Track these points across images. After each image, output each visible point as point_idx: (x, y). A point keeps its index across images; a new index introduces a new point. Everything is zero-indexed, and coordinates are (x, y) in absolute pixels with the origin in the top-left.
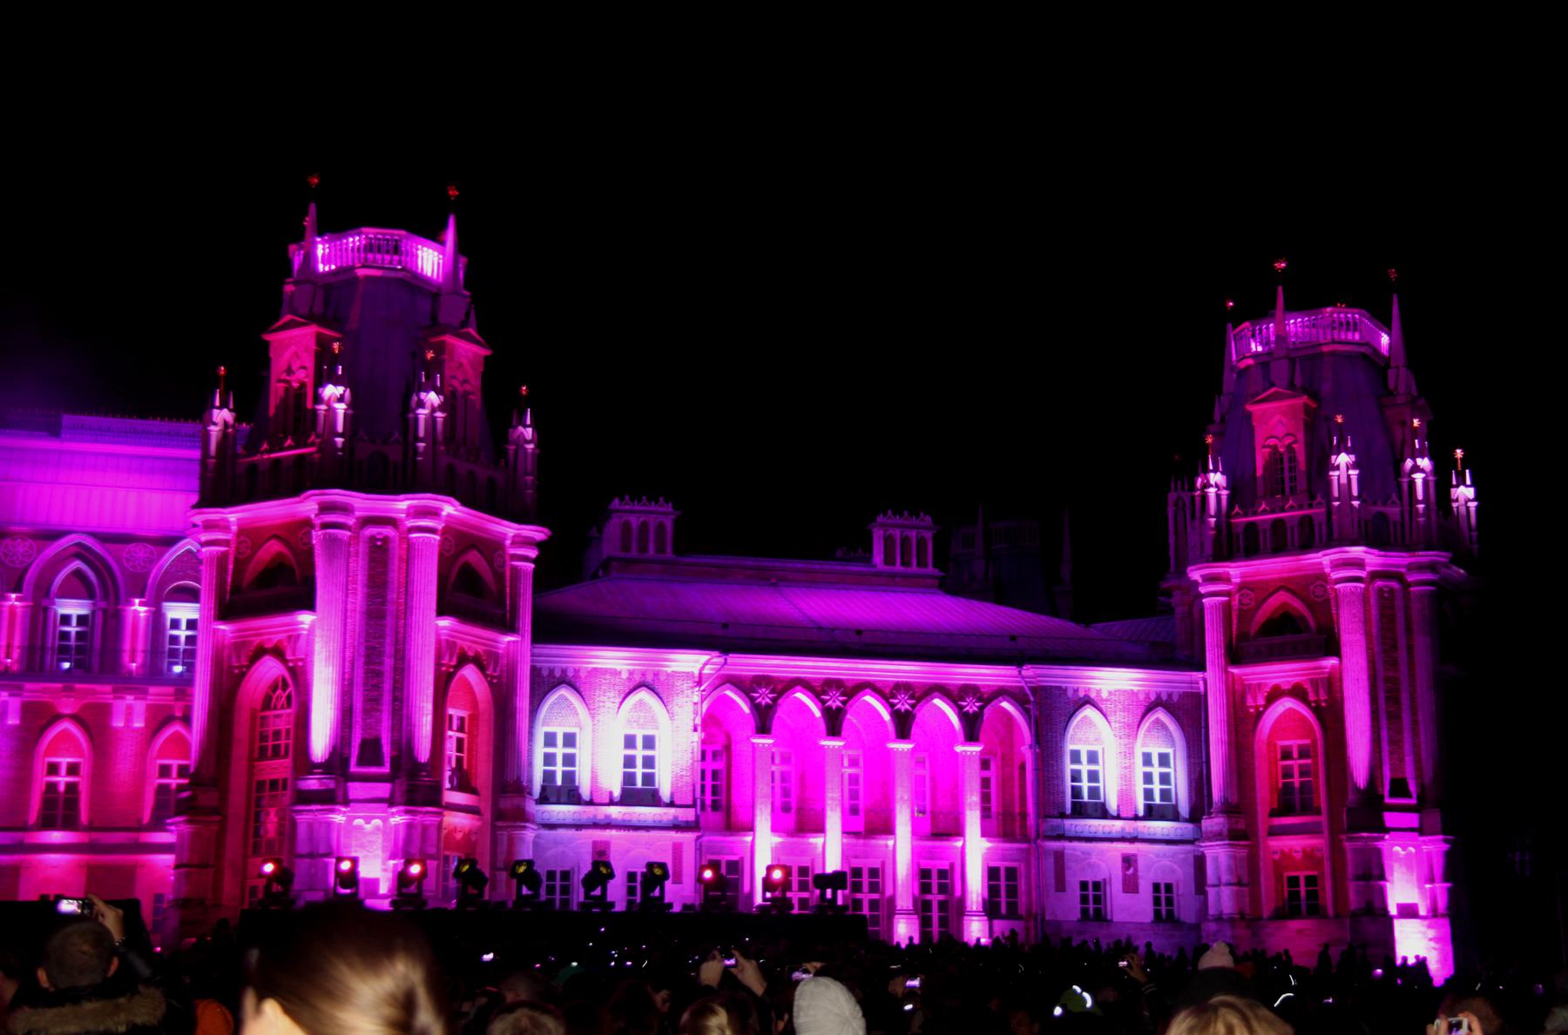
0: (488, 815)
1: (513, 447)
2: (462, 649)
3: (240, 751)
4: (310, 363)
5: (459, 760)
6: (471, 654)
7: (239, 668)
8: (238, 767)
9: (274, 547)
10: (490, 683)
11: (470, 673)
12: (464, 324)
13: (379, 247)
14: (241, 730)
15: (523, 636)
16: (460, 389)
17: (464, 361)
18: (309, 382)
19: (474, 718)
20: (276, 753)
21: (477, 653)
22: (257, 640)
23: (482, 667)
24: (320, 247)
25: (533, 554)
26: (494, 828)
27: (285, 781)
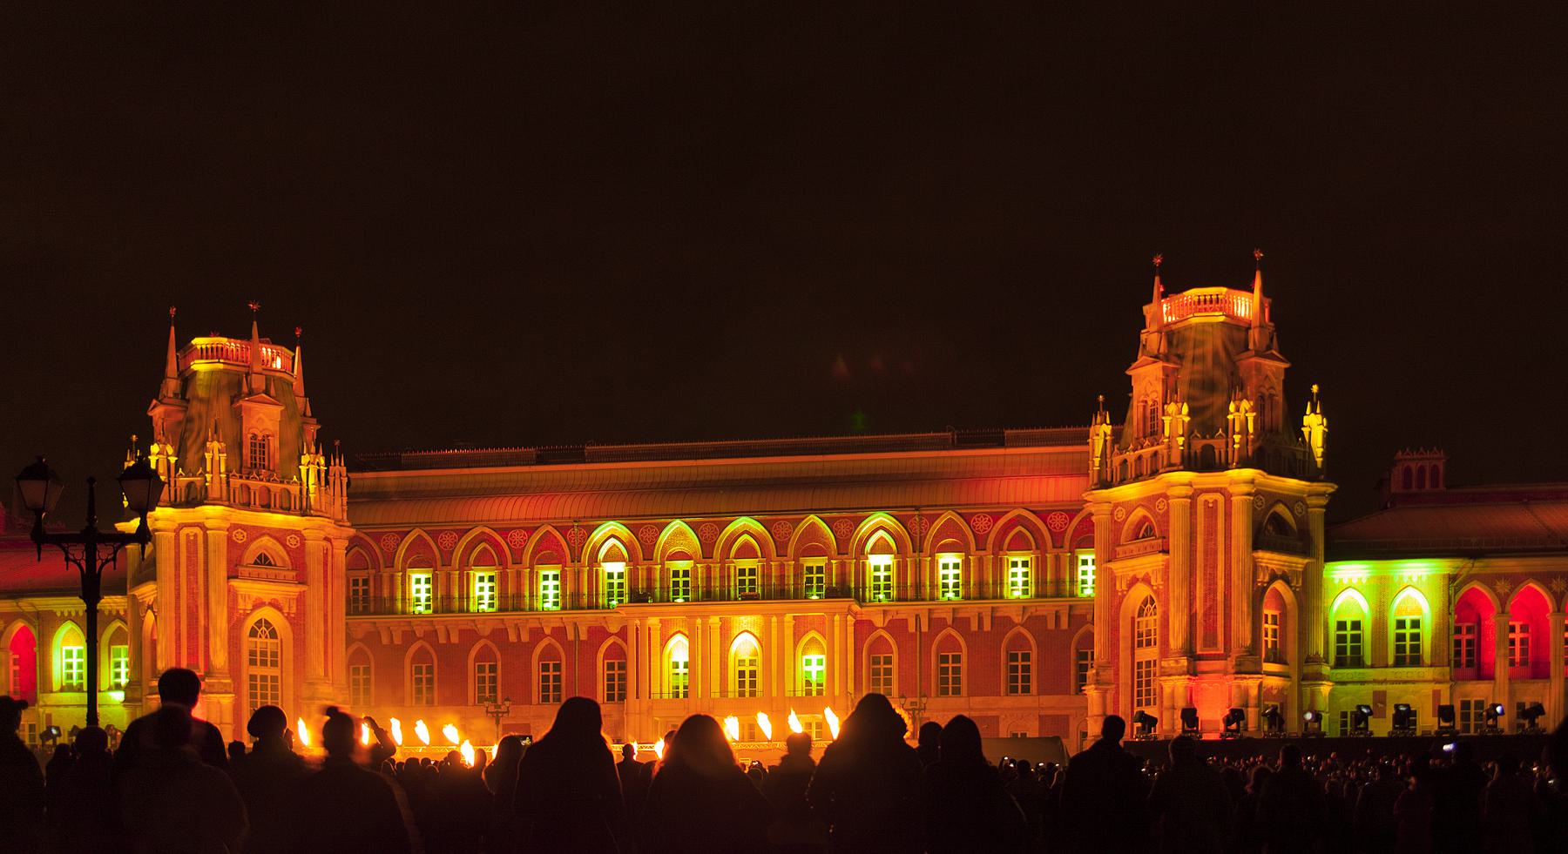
0: (1295, 678)
1: (1308, 429)
2: (1273, 570)
3: (1124, 645)
4: (1160, 388)
5: (1274, 643)
6: (1279, 573)
7: (1123, 591)
8: (1124, 655)
9: (1140, 512)
10: (1294, 592)
11: (1279, 585)
12: (1269, 348)
13: (1205, 300)
14: (1124, 631)
15: (1318, 559)
16: (1267, 394)
17: (1269, 373)
18: (1159, 400)
19: (1284, 614)
20: (1149, 644)
21: (1284, 572)
22: (1131, 574)
23: (1287, 581)
24: (1165, 305)
25: (1323, 502)
26: (1300, 685)
27: (1155, 661)
